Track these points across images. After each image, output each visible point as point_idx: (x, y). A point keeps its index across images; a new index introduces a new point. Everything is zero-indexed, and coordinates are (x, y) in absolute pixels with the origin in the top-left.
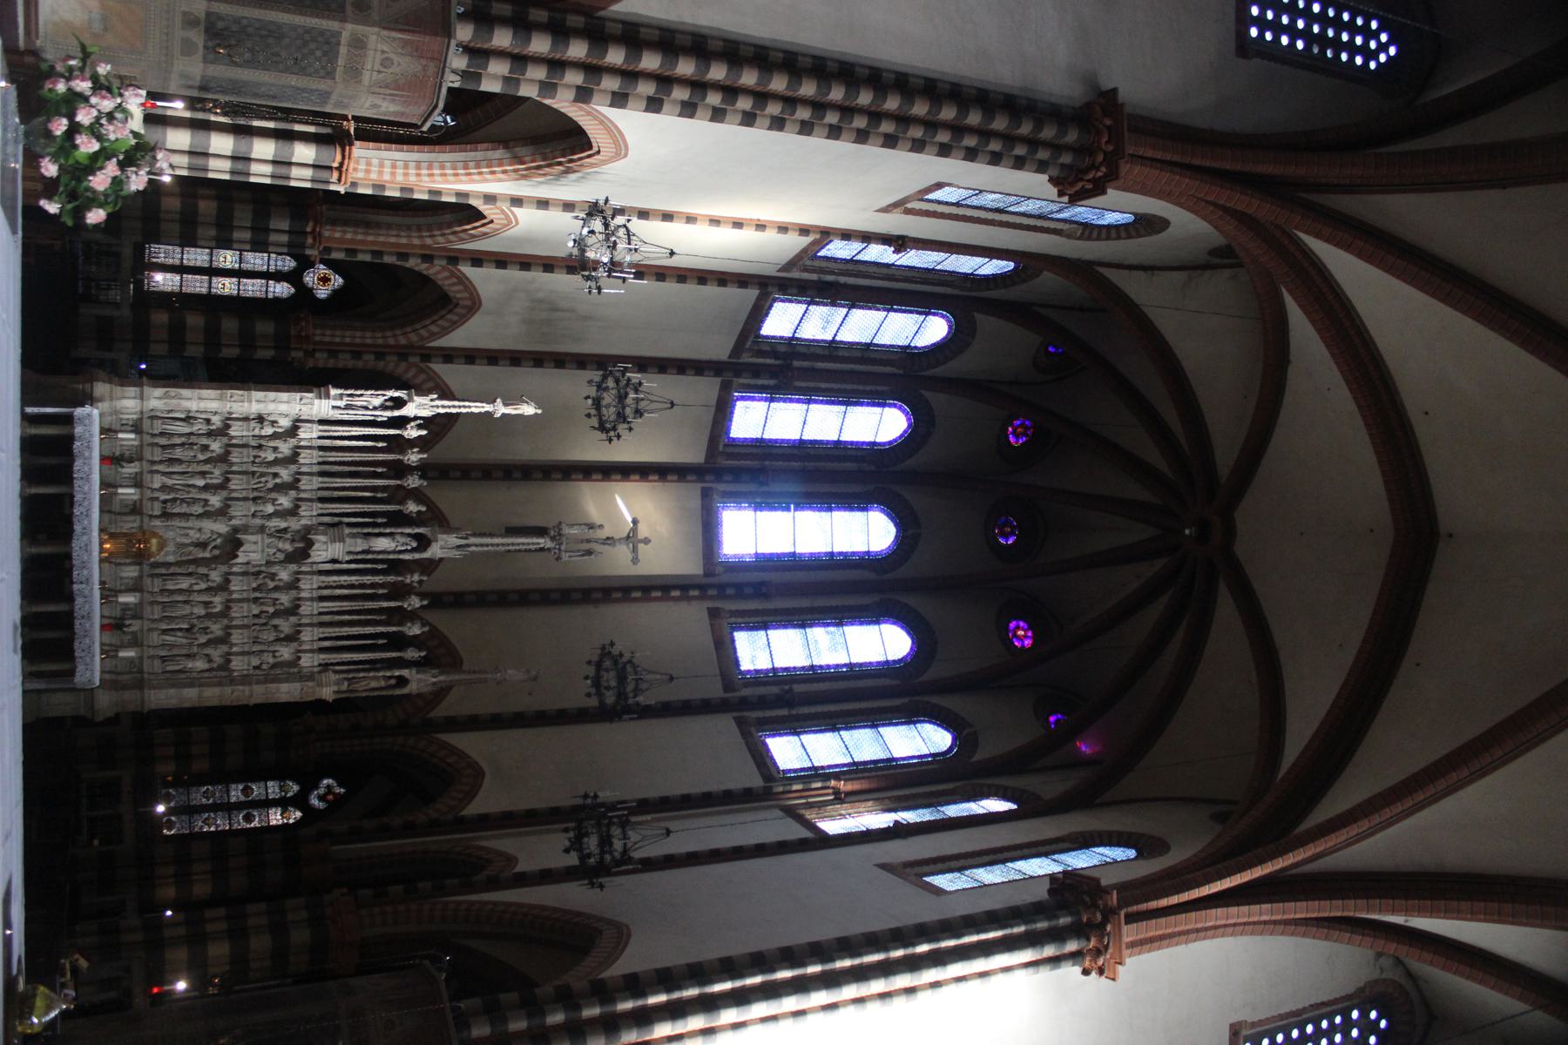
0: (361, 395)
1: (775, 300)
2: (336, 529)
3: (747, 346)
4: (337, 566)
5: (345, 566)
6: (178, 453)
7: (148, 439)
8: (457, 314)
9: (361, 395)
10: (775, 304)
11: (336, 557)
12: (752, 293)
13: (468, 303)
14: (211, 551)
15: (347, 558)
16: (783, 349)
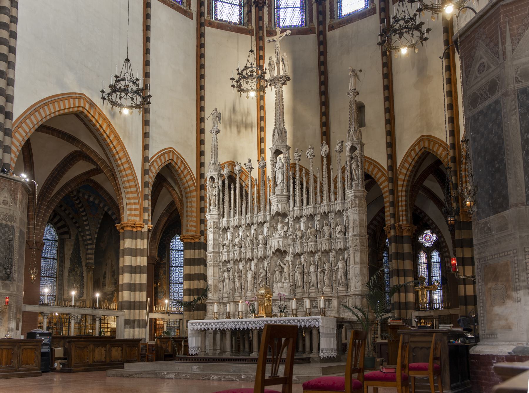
0: (210, 199)
1: (216, 19)
2: (272, 201)
3: (246, 27)
4: (291, 198)
5: (291, 193)
6: (237, 284)
7: (232, 299)
8: (177, 161)
9: (210, 199)
10: (219, 18)
11: (286, 199)
12: (208, 30)
13: (171, 154)
14: (285, 265)
15: (285, 192)
16: (246, 9)
